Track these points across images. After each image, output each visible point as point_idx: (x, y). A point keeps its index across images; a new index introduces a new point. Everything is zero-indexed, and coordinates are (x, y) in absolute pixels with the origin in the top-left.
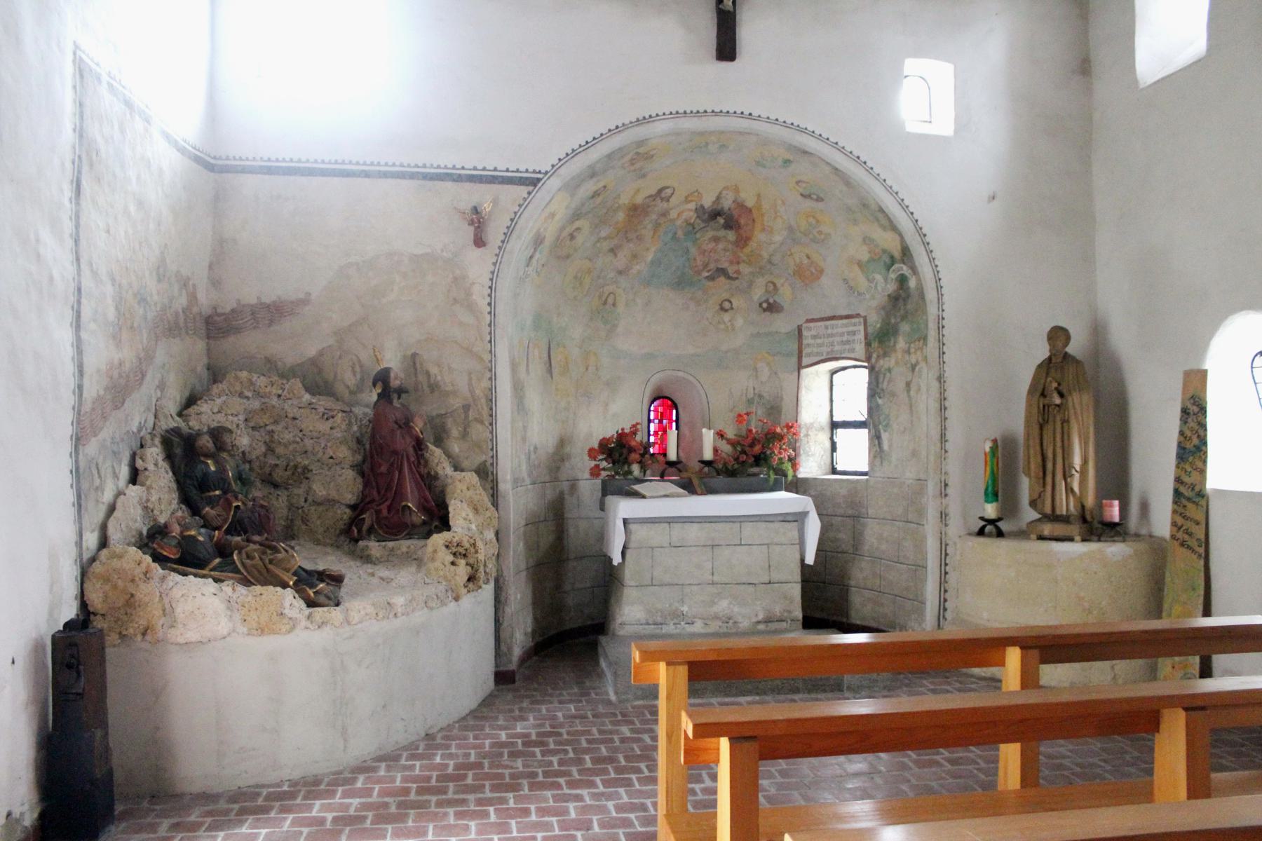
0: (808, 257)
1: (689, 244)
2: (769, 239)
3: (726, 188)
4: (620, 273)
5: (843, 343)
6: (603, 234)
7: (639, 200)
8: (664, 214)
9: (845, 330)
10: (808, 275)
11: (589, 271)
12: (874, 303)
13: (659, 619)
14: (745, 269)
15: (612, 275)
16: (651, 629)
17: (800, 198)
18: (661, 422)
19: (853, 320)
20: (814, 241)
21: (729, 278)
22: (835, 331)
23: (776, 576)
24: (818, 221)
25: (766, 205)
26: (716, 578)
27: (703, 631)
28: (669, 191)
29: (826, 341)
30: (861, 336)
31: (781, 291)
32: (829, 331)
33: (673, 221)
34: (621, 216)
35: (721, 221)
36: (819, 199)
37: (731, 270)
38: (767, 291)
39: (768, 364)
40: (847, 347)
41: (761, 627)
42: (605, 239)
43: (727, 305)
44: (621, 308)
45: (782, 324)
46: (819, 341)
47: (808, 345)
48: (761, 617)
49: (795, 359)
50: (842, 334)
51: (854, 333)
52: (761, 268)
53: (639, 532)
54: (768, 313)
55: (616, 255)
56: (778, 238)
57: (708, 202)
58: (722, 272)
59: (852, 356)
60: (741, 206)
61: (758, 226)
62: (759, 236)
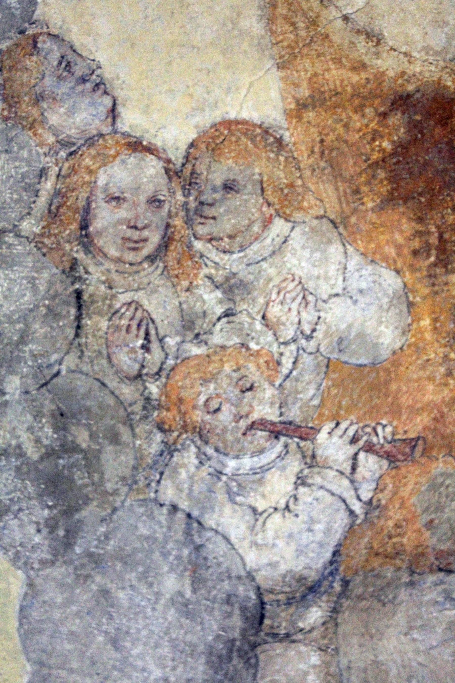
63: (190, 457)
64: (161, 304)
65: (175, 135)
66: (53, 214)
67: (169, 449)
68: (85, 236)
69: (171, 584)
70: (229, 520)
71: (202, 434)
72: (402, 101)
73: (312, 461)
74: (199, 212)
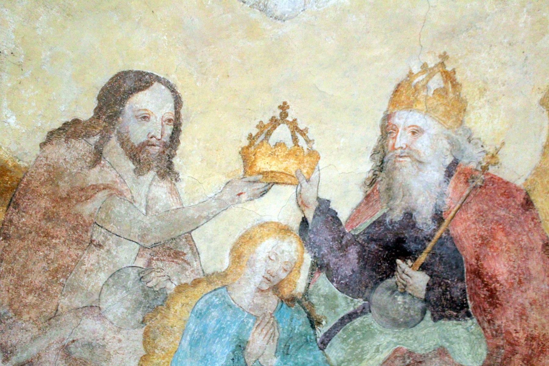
3: (403, 94)
8: (172, 247)
28: (151, 103)
33: (219, 280)
35: (414, 278)
60: (480, 184)
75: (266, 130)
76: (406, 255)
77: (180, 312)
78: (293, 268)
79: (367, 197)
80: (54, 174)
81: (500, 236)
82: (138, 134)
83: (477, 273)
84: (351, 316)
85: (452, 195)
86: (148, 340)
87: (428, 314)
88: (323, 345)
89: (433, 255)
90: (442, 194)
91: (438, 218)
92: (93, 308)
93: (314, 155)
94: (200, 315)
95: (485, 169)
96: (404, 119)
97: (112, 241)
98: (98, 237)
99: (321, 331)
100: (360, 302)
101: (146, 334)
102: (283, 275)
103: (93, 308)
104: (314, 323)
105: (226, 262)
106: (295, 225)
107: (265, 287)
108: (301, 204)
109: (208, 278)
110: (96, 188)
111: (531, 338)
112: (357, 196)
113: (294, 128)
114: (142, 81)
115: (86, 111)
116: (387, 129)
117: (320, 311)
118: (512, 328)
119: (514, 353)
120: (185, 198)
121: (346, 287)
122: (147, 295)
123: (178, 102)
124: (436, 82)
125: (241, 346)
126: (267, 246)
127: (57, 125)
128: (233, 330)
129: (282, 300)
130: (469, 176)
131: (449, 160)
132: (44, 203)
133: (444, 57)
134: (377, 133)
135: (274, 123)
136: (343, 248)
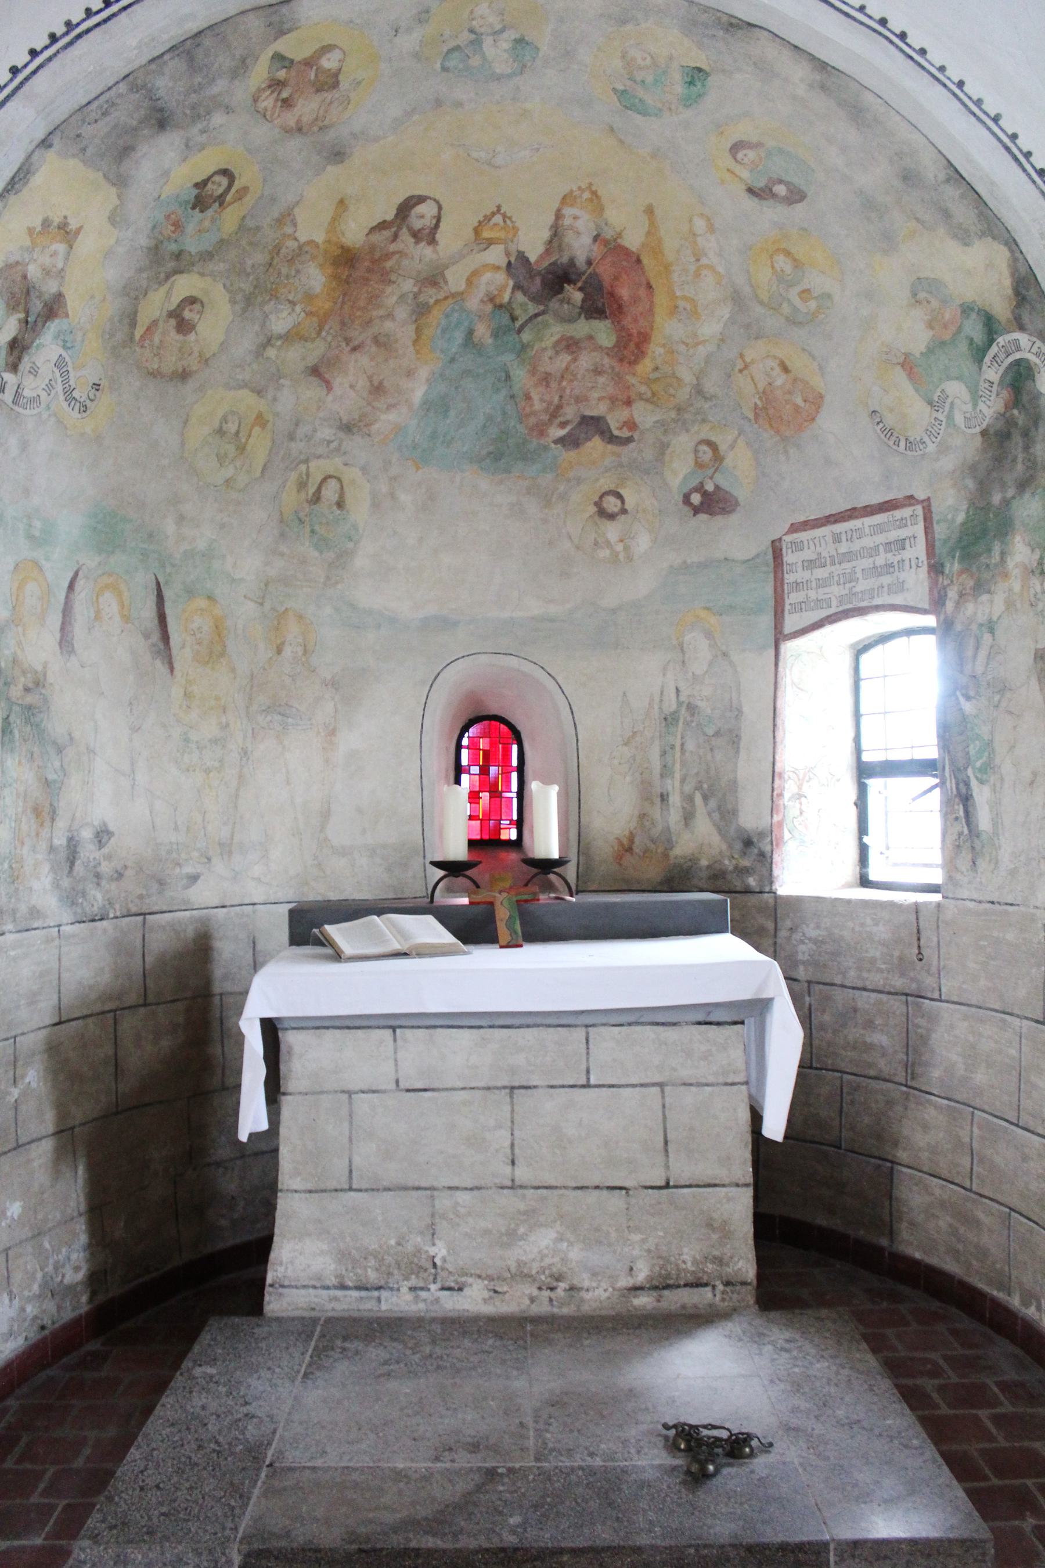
0: (786, 369)
1: (508, 358)
2: (691, 331)
3: (567, 199)
4: (348, 428)
5: (876, 571)
6: (282, 321)
7: (354, 232)
8: (433, 279)
9: (880, 539)
10: (785, 414)
11: (260, 420)
12: (948, 463)
13: (372, 1276)
14: (645, 415)
15: (326, 433)
16: (349, 1303)
17: (750, 204)
18: (484, 771)
19: (898, 514)
20: (793, 321)
21: (612, 439)
22: (857, 546)
23: (682, 1169)
24: (797, 264)
25: (670, 244)
26: (523, 1174)
27: (488, 1309)
28: (427, 210)
29: (837, 569)
30: (919, 550)
31: (728, 462)
32: (843, 548)
34: (315, 278)
36: (796, 196)
37: (613, 425)
38: (699, 465)
39: (709, 635)
40: (886, 580)
41: (644, 1301)
42: (290, 337)
43: (611, 504)
44: (359, 511)
45: (737, 539)
46: (820, 573)
47: (797, 586)
48: (641, 1276)
49: (766, 620)
50: (874, 551)
51: (901, 544)
52: (679, 409)
53: (304, 1055)
54: (703, 517)
55: (328, 385)
56: (710, 328)
57: (533, 244)
58: (593, 425)
59: (898, 600)
60: (613, 248)
61: (661, 299)
62: (667, 329)
63: (272, 303)
64: (284, 271)
65: (303, 239)
66: (275, 246)
67: (270, 300)
68: (278, 254)
69: (257, 328)
70: (272, 317)
71: (277, 298)
72: (342, 247)
73: (293, 310)
74: (299, 255)
75: (488, 218)
76: (570, 282)
77: (436, 316)
78: (502, 289)
79: (547, 250)
80: (372, 248)
81: (625, 277)
82: (417, 224)
83: (612, 294)
84: (536, 315)
85: (597, 251)
86: (418, 331)
87: (583, 316)
88: (519, 331)
89: (585, 282)
90: (591, 250)
91: (589, 263)
92: (390, 316)
93: (515, 229)
94: (447, 316)
95: (615, 240)
96: (568, 211)
97: (400, 280)
98: (393, 277)
99: (518, 324)
100: (542, 308)
101: (417, 328)
102: (496, 293)
103: (390, 316)
104: (514, 319)
105: (462, 287)
106: (504, 265)
107: (485, 299)
108: (508, 254)
109: (453, 295)
110: (394, 253)
111: (640, 333)
112: (540, 249)
113: (504, 216)
114: (421, 199)
115: (390, 216)
116: (559, 216)
117: (518, 312)
118: (630, 327)
119: (630, 340)
120: (441, 254)
121: (534, 299)
122: (418, 306)
123: (440, 208)
124: (587, 195)
125: (470, 333)
126: (488, 276)
127: (375, 224)
128: (466, 324)
129: (495, 306)
130: (606, 242)
131: (595, 233)
132: (366, 264)
133: (591, 184)
134: (553, 218)
135: (493, 214)
136: (532, 277)
